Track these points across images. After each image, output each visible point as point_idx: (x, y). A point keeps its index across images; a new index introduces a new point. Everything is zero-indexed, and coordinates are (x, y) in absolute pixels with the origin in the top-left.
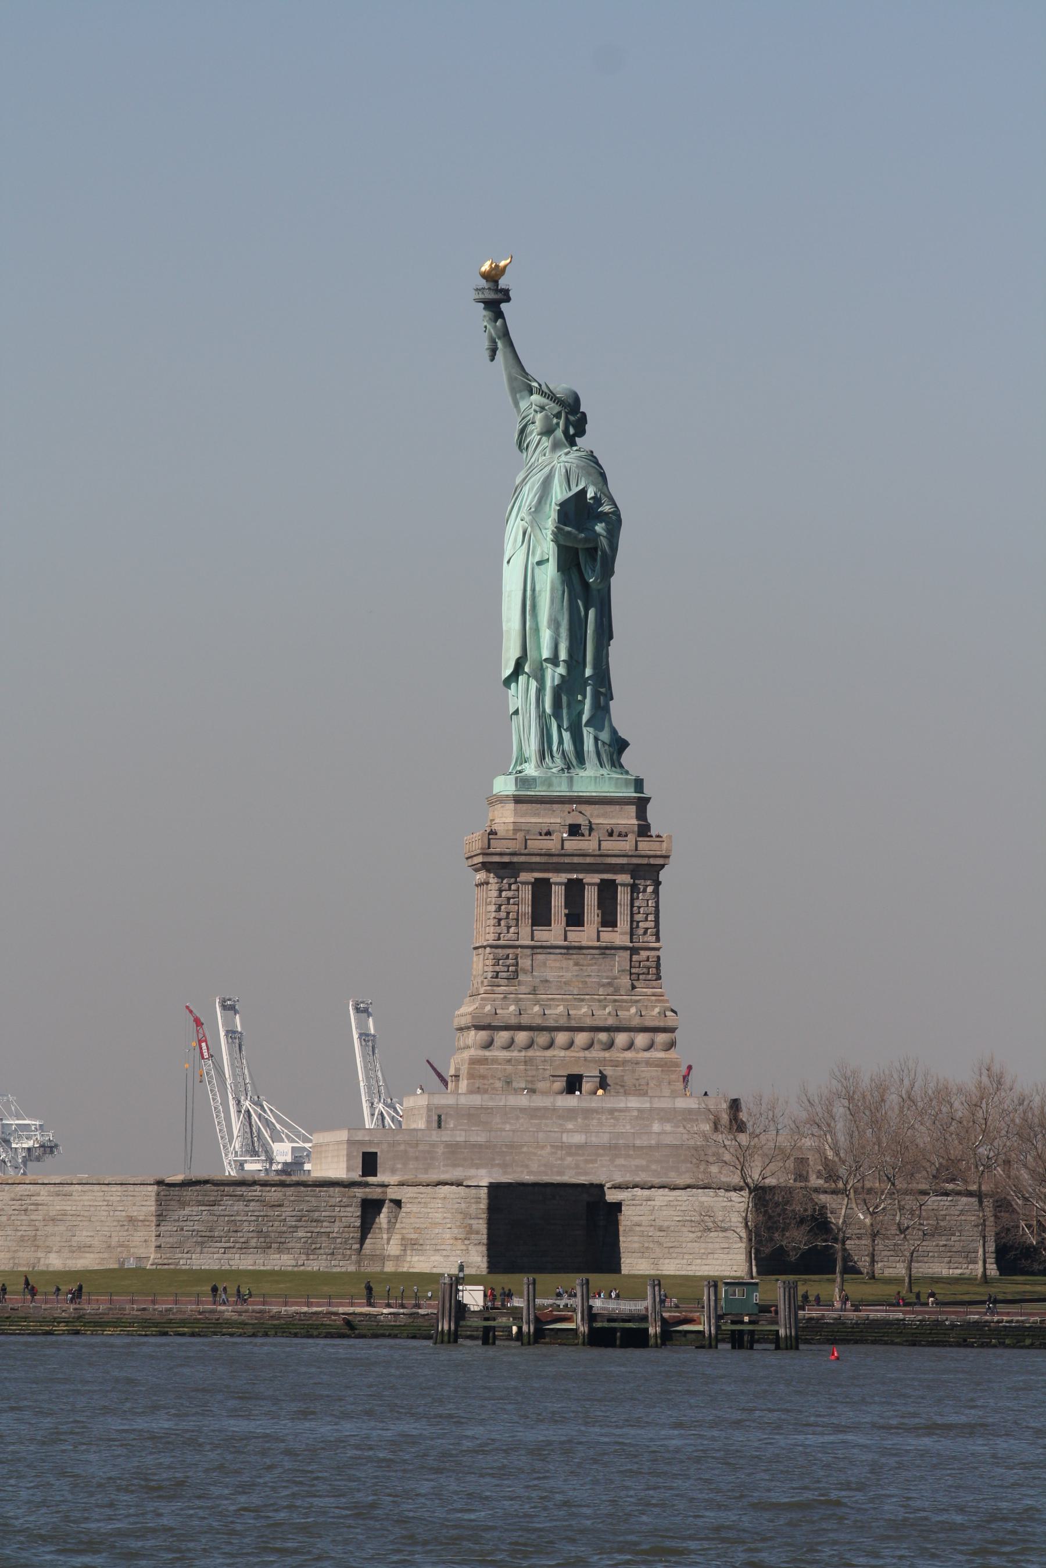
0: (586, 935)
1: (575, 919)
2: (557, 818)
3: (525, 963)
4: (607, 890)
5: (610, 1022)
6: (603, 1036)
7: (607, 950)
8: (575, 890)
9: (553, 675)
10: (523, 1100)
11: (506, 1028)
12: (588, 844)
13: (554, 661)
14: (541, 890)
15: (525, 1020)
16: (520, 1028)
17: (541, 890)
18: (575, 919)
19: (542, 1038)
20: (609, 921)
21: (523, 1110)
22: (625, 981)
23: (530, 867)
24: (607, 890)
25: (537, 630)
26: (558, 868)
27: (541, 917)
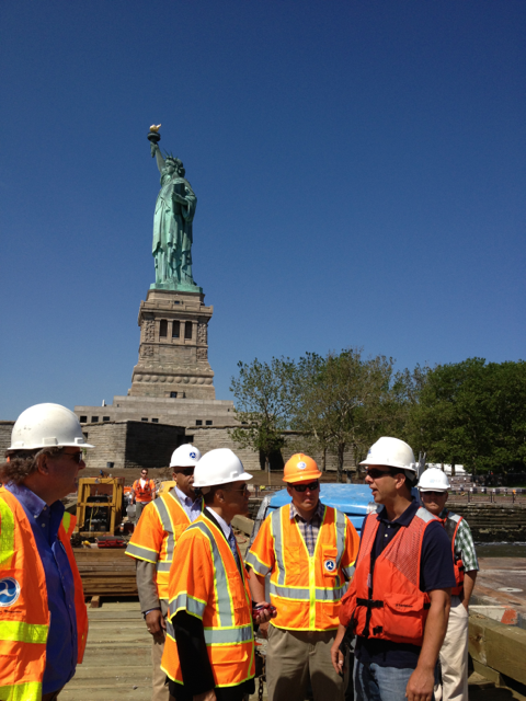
0: (181, 340)
1: (176, 334)
2: (171, 298)
3: (156, 350)
4: (188, 325)
5: (188, 372)
6: (185, 378)
7: (188, 347)
8: (176, 325)
9: (170, 251)
10: (153, 400)
11: (148, 373)
12: (182, 308)
13: (170, 244)
14: (164, 324)
15: (155, 371)
16: (153, 374)
17: (164, 324)
18: (176, 334)
19: (162, 378)
20: (188, 335)
21: (153, 403)
22: (194, 358)
23: (160, 315)
24: (188, 325)
25: (165, 234)
26: (171, 316)
27: (163, 333)
